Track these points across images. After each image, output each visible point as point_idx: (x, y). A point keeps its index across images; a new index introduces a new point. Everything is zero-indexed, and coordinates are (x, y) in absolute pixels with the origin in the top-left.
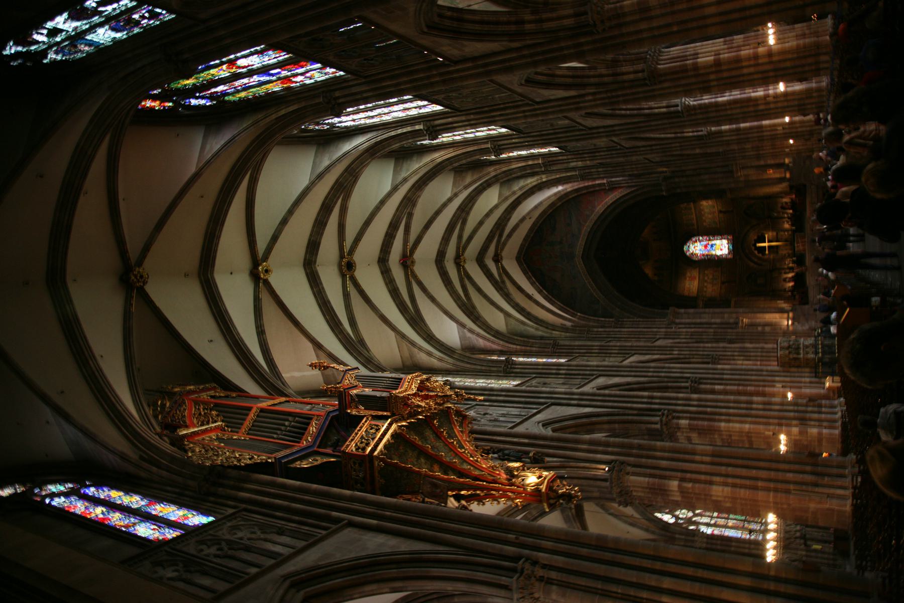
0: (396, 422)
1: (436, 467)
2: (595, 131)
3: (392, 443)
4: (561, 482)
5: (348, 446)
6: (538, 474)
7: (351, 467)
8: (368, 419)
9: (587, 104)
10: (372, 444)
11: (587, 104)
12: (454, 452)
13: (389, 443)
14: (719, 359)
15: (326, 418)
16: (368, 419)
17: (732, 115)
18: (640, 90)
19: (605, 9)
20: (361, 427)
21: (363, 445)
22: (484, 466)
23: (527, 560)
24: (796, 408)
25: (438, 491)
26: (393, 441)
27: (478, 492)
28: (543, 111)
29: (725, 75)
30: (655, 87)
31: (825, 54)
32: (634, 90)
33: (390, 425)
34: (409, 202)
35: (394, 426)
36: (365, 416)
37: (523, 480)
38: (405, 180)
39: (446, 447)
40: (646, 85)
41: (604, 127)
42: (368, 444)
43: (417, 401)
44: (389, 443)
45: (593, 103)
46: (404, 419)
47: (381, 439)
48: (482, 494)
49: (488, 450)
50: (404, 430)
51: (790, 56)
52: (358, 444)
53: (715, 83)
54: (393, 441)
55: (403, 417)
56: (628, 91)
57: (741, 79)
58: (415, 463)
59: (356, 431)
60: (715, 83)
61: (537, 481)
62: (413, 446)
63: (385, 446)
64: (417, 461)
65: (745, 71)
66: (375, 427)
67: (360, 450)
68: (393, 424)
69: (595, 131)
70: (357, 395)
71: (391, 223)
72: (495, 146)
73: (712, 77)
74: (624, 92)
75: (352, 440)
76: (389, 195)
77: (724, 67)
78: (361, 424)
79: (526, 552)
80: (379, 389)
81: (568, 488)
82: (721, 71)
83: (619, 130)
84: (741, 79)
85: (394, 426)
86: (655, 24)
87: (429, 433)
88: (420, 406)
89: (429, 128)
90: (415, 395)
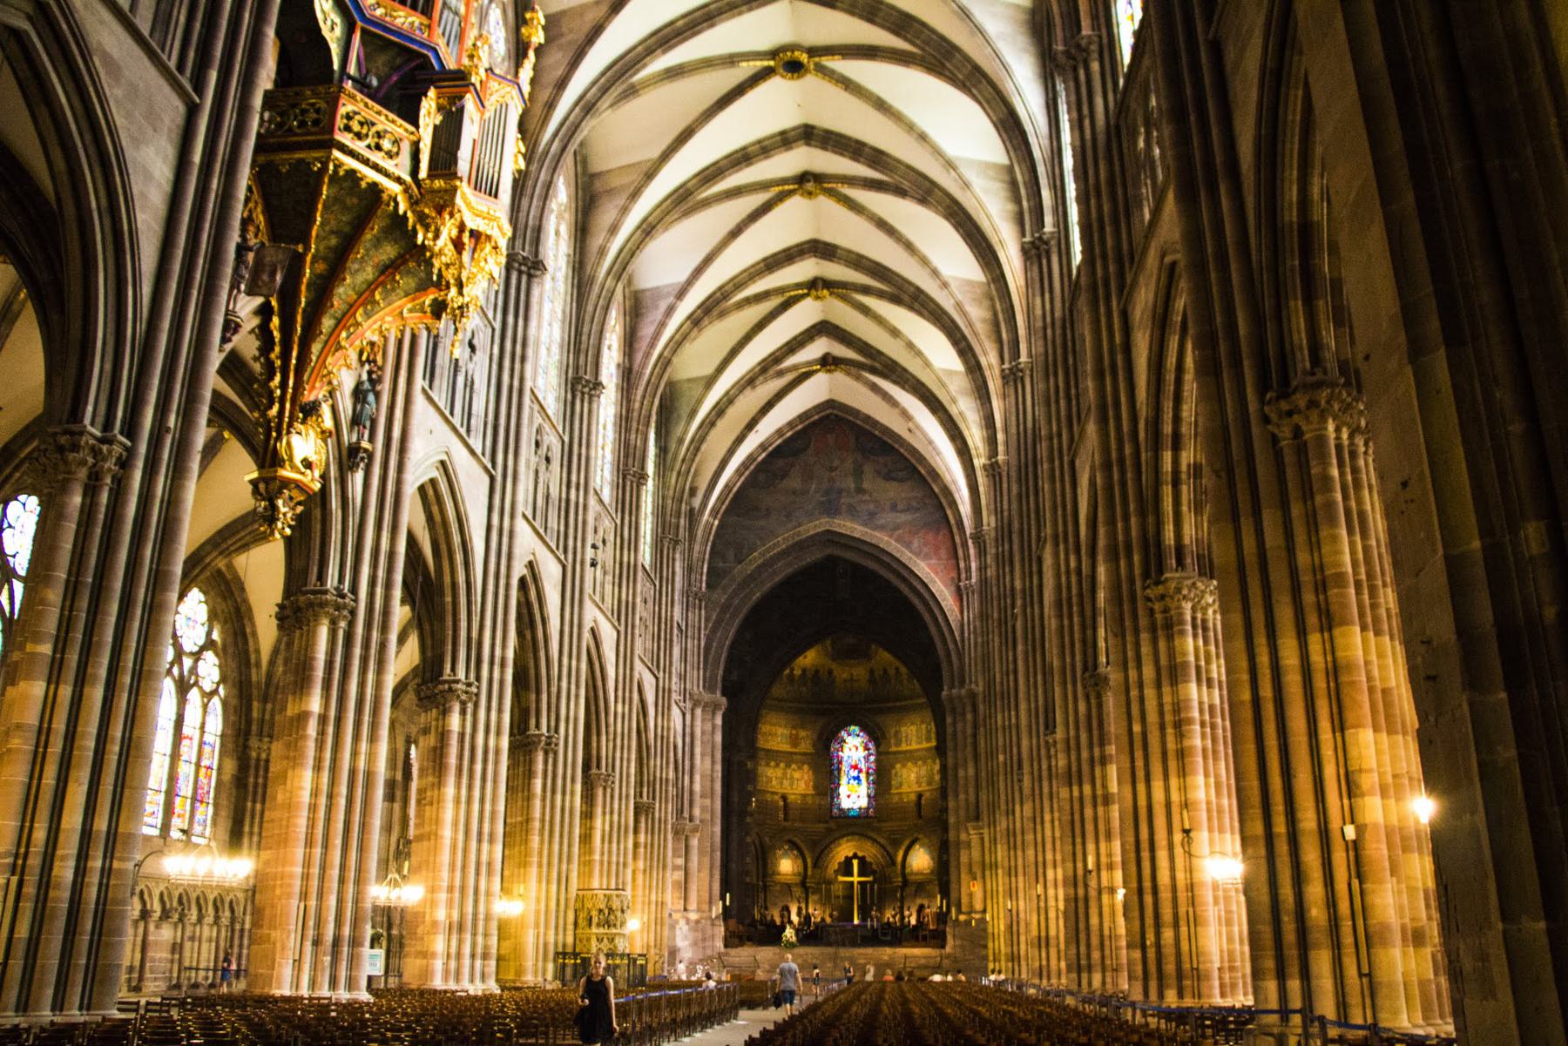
0: (406, 190)
1: (321, 267)
2: (1035, 569)
3: (359, 186)
4: (299, 503)
5: (353, 97)
6: (313, 458)
7: (313, 105)
8: (412, 133)
9: (1062, 556)
10: (359, 146)
11: (1062, 556)
12: (356, 301)
13: (362, 179)
14: (605, 789)
15: (422, 45)
16: (412, 133)
17: (1042, 823)
18: (1078, 658)
19: (1183, 604)
20: (393, 122)
21: (356, 127)
22: (329, 360)
23: (127, 449)
24: (481, 916)
25: (265, 277)
26: (363, 185)
27: (277, 349)
28: (1057, 473)
29: (1088, 812)
30: (1079, 685)
31: (1104, 983)
32: (1077, 646)
33: (399, 180)
34: (924, 191)
35: (395, 188)
36: (417, 126)
37: (300, 433)
38: (966, 185)
39: (365, 286)
40: (1085, 669)
41: (1041, 586)
42: (359, 136)
43: (448, 229)
44: (362, 179)
45: (1063, 569)
46: (414, 203)
47: (366, 162)
48: (273, 356)
49: (375, 361)
50: (388, 205)
51: (1106, 925)
52: (357, 117)
53: (1076, 793)
54: (363, 185)
55: (417, 203)
56: (1077, 636)
57: (1078, 840)
58: (327, 228)
59: (385, 111)
60: (1076, 793)
61: (297, 460)
62: (359, 225)
63: (352, 173)
64: (332, 232)
65: (1091, 847)
66: (395, 150)
67: (345, 121)
68: (401, 184)
69: (1035, 569)
70: (461, 110)
71: (881, 152)
72: (1021, 371)
73: (1087, 789)
74: (1076, 628)
75: (366, 105)
76: (937, 152)
77: (1100, 810)
78: (400, 121)
79: (143, 448)
80: (477, 153)
81: (289, 515)
82: (1095, 806)
83: (1033, 613)
84: (1078, 840)
85: (395, 188)
86: (1150, 693)
87: (389, 251)
88: (437, 236)
89: (1046, 243)
90: (462, 227)
